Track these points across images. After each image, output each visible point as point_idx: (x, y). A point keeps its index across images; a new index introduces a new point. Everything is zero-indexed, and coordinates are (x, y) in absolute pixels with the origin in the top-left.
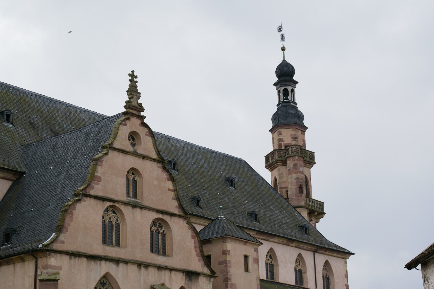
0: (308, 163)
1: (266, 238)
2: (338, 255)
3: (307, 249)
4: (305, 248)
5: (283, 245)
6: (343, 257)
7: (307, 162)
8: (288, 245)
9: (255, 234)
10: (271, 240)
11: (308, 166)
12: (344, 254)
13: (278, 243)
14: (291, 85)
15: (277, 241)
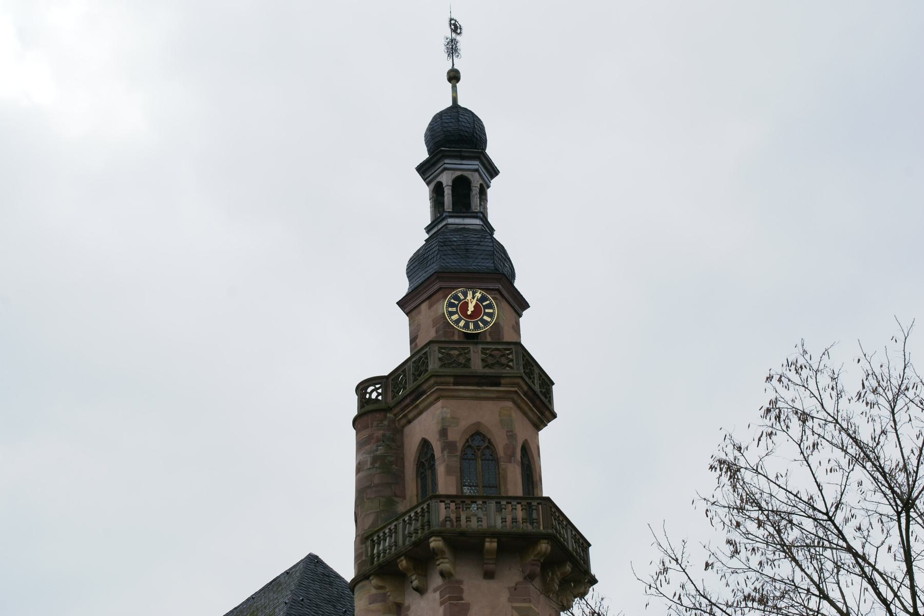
0: (413, 396)
7: (408, 401)
14: (446, 166)
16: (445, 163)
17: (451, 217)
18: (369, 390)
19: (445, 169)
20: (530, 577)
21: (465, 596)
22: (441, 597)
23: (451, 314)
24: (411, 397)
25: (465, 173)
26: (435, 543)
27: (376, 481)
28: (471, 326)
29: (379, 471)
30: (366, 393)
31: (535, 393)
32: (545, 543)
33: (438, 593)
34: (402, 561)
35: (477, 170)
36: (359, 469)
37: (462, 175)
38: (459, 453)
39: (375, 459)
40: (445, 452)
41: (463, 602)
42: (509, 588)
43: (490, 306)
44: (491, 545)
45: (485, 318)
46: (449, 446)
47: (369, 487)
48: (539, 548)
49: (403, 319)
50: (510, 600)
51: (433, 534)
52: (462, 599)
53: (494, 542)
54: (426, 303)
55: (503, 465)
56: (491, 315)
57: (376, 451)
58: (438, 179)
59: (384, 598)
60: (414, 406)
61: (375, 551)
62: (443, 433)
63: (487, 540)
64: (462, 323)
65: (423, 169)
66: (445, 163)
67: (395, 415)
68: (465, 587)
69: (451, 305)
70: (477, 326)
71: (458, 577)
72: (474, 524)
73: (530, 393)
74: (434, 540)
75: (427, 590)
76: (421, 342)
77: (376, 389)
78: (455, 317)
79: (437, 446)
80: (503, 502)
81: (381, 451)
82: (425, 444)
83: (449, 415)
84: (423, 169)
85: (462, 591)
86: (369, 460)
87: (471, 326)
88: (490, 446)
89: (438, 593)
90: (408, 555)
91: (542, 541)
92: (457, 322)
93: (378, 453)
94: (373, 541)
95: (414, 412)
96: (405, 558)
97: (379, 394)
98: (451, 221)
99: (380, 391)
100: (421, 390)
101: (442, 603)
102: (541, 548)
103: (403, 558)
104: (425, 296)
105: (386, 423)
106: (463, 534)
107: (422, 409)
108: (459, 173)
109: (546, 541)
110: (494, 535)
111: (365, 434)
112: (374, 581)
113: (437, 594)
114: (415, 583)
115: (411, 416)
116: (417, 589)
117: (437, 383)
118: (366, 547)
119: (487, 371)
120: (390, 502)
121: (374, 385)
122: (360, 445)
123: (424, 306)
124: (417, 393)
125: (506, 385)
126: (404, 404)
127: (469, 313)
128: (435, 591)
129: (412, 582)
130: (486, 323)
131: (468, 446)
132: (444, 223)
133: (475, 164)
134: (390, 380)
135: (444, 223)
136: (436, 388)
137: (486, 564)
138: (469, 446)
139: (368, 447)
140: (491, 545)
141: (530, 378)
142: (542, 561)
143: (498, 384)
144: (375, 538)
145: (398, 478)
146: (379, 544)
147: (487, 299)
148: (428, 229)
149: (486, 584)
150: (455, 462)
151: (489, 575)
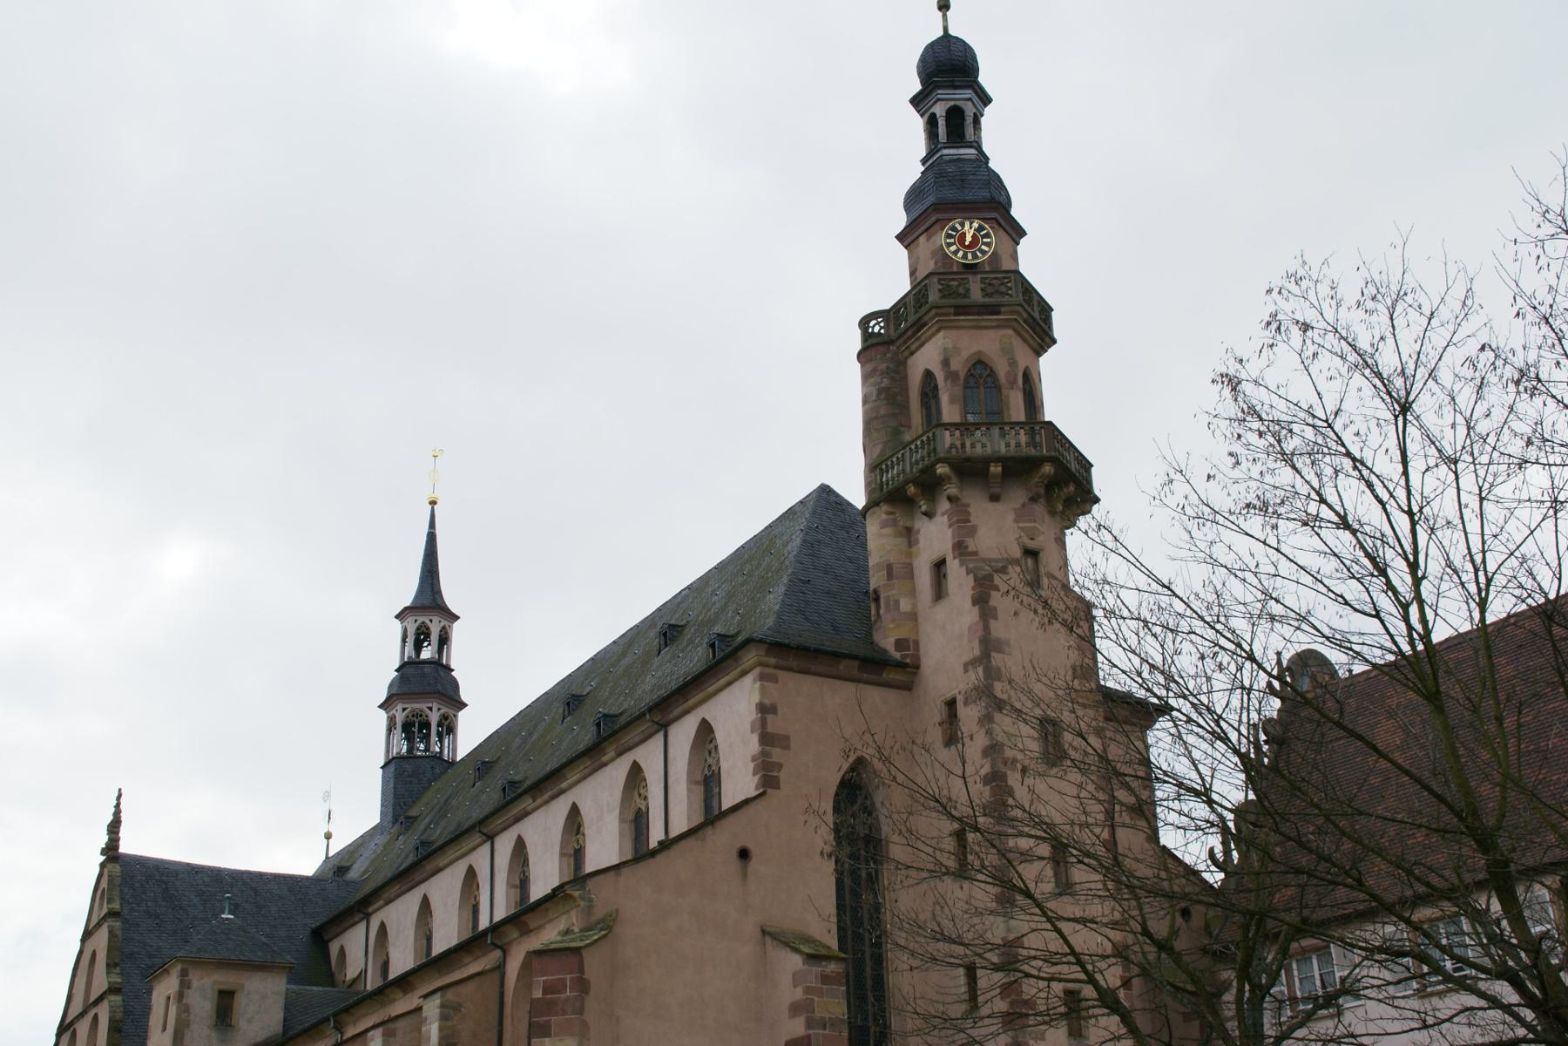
0: (915, 328)
1: (555, 791)
2: (723, 681)
3: (642, 737)
4: (637, 739)
5: (595, 774)
6: (739, 669)
7: (910, 333)
8: (605, 765)
9: (531, 801)
10: (564, 785)
11: (927, 335)
12: (736, 661)
13: (584, 778)
15: (575, 778)
17: (945, 148)
18: (872, 324)
19: (939, 100)
20: (1033, 499)
21: (972, 518)
22: (949, 520)
23: (949, 245)
25: (958, 103)
26: (941, 469)
27: (882, 412)
28: (970, 256)
29: (884, 402)
30: (869, 327)
31: (1035, 320)
33: (946, 517)
35: (970, 99)
36: (865, 402)
37: (955, 107)
38: (962, 382)
39: (880, 391)
40: (949, 382)
42: (1015, 510)
43: (987, 235)
44: (996, 469)
45: (983, 247)
46: (952, 376)
47: (876, 418)
49: (902, 253)
50: (1016, 521)
51: (940, 461)
52: (969, 522)
54: (925, 235)
55: (1005, 392)
56: (988, 244)
58: (932, 111)
59: (894, 523)
61: (884, 479)
62: (946, 363)
64: (960, 254)
65: (917, 101)
67: (898, 347)
68: (972, 510)
69: (949, 236)
70: (975, 256)
71: (965, 501)
72: (979, 450)
73: (1030, 321)
76: (921, 275)
77: (878, 323)
78: (953, 248)
79: (940, 376)
80: (1007, 428)
81: (886, 382)
82: (928, 375)
83: (950, 346)
84: (917, 101)
85: (969, 514)
86: (875, 393)
87: (970, 256)
88: (992, 373)
89: (946, 517)
90: (916, 482)
92: (956, 253)
93: (883, 385)
94: (881, 469)
95: (917, 344)
97: (881, 328)
98: (945, 152)
99: (882, 324)
100: (922, 322)
101: (950, 526)
104: (923, 228)
105: (889, 355)
106: (968, 460)
108: (952, 103)
110: (999, 459)
111: (870, 367)
112: (885, 507)
114: (924, 508)
115: (913, 347)
116: (925, 514)
117: (937, 314)
118: (876, 476)
119: (987, 300)
120: (896, 432)
121: (876, 319)
122: (866, 378)
123: (922, 239)
124: (919, 325)
125: (1005, 313)
126: (906, 336)
127: (967, 243)
128: (943, 514)
130: (983, 253)
131: (970, 375)
132: (939, 154)
133: (968, 93)
135: (939, 154)
138: (972, 375)
139: (872, 380)
140: (996, 469)
141: (1029, 305)
144: (884, 467)
145: (904, 408)
146: (888, 472)
147: (984, 229)
148: (924, 161)
150: (958, 391)
151: (995, 498)
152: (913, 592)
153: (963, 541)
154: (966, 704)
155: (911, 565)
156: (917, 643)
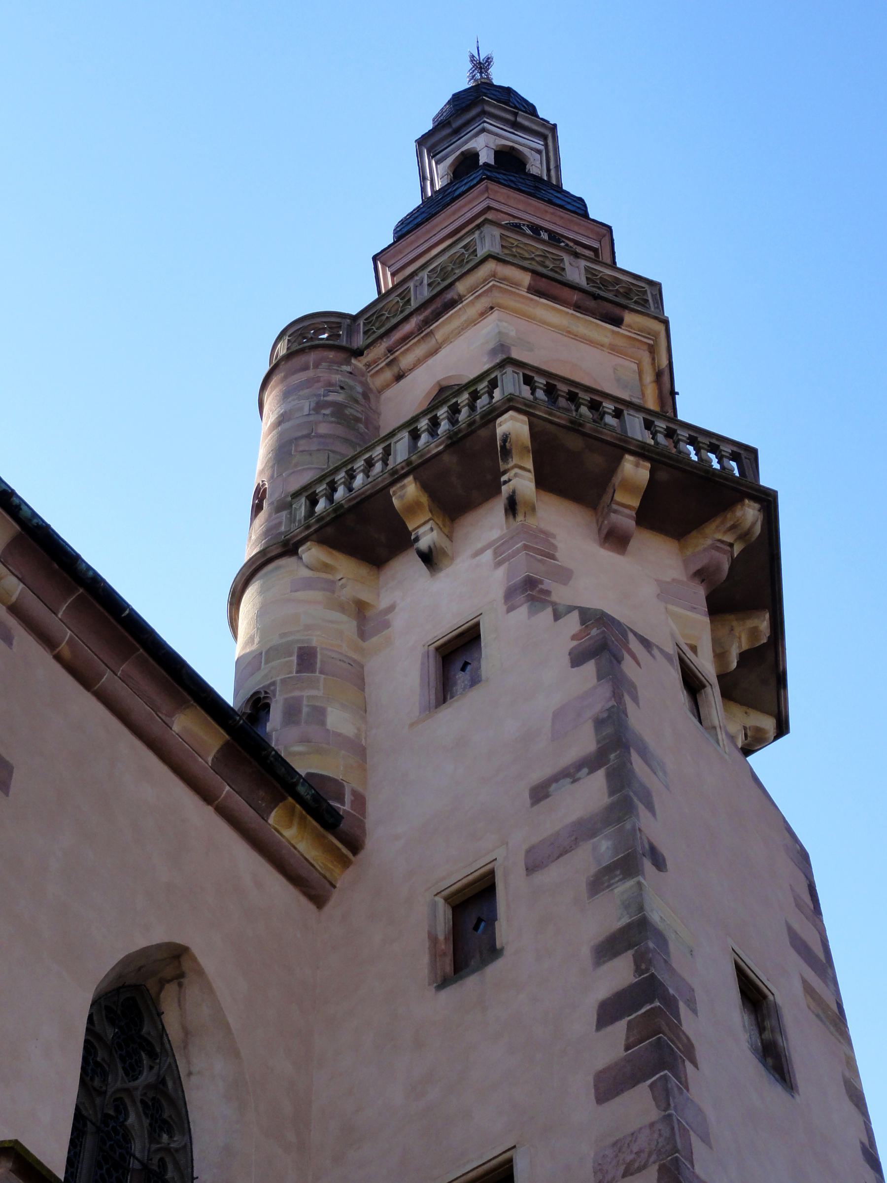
16: (485, 122)
19: (484, 130)
24: (421, 317)
27: (323, 429)
32: (754, 509)
34: (404, 487)
35: (539, 152)
37: (513, 148)
39: (319, 407)
41: (556, 562)
48: (739, 513)
52: (553, 557)
53: (644, 467)
57: (324, 396)
59: (331, 587)
60: (422, 335)
63: (628, 457)
66: (485, 122)
74: (512, 418)
75: (452, 559)
85: (555, 547)
91: (747, 501)
95: (420, 351)
96: (415, 479)
100: (450, 295)
102: (744, 515)
103: (410, 479)
107: (440, 341)
109: (757, 506)
112: (311, 553)
113: (488, 555)
114: (424, 544)
115: (406, 361)
129: (417, 539)
134: (361, 322)
136: (491, 284)
137: (615, 512)
142: (737, 549)
143: (617, 321)
149: (607, 556)
152: (362, 709)
153: (541, 582)
154: (532, 868)
155: (362, 667)
156: (360, 800)
